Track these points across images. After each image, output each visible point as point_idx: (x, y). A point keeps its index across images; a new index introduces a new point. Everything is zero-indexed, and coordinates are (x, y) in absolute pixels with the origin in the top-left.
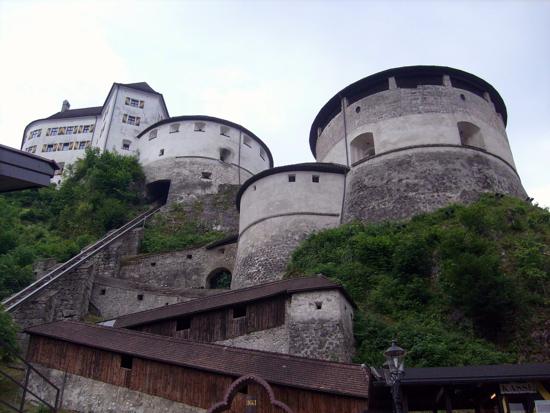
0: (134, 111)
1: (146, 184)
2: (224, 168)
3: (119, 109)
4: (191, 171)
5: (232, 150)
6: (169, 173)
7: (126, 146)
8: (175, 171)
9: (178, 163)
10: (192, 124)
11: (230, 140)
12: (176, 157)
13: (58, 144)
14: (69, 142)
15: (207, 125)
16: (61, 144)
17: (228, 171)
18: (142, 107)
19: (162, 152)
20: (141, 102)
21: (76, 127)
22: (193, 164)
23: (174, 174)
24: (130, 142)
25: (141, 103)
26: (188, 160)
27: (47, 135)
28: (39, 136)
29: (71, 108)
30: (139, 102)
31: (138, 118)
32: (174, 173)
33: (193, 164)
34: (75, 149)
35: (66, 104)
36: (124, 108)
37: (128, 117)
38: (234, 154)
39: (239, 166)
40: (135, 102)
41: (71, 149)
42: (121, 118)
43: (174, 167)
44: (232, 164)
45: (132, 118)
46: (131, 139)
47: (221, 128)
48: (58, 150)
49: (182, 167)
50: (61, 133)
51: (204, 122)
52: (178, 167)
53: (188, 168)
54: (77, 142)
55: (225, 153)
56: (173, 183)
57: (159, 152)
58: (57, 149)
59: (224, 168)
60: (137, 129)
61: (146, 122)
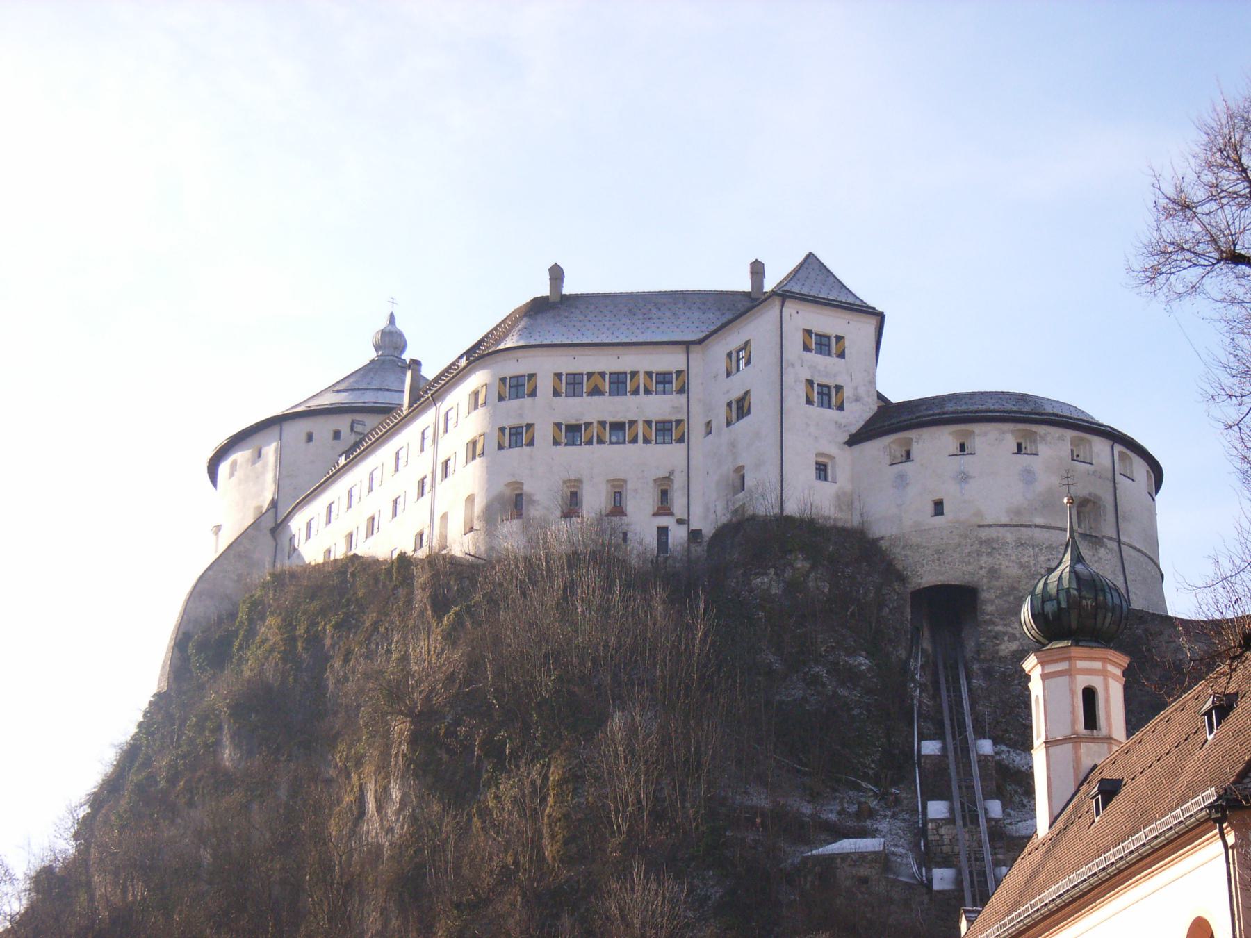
0: (826, 367)
1: (909, 590)
2: (1091, 554)
3: (793, 365)
4: (1021, 565)
5: (1100, 499)
6: (971, 569)
7: (822, 470)
8: (982, 563)
9: (988, 542)
10: (1004, 433)
11: (1094, 473)
12: (980, 526)
13: (595, 424)
14: (622, 420)
15: (1040, 437)
16: (602, 424)
17: (1100, 558)
18: (841, 355)
19: (938, 507)
20: (839, 338)
21: (634, 374)
22: (1022, 544)
23: (982, 572)
24: (832, 458)
25: (837, 343)
26: (1009, 536)
27: (556, 393)
28: (533, 394)
29: (568, 289)
30: (833, 341)
31: (839, 388)
32: (981, 568)
33: (1021, 544)
34: (647, 441)
35: (556, 274)
36: (802, 361)
37: (815, 386)
38: (1105, 506)
39: (1119, 542)
40: (821, 343)
41: (634, 440)
42: (801, 390)
43: (979, 554)
44: (1104, 537)
45: (825, 391)
46: (833, 450)
47: (1074, 442)
48: (598, 443)
49: (1000, 554)
50: (596, 391)
51: (1034, 427)
52: (989, 554)
53: (1014, 558)
54: (648, 423)
55: (1084, 506)
56: (985, 595)
57: (930, 508)
58: (595, 439)
59: (1091, 554)
60: (843, 421)
61: (857, 399)
